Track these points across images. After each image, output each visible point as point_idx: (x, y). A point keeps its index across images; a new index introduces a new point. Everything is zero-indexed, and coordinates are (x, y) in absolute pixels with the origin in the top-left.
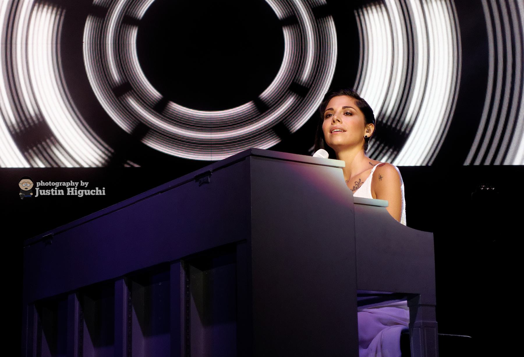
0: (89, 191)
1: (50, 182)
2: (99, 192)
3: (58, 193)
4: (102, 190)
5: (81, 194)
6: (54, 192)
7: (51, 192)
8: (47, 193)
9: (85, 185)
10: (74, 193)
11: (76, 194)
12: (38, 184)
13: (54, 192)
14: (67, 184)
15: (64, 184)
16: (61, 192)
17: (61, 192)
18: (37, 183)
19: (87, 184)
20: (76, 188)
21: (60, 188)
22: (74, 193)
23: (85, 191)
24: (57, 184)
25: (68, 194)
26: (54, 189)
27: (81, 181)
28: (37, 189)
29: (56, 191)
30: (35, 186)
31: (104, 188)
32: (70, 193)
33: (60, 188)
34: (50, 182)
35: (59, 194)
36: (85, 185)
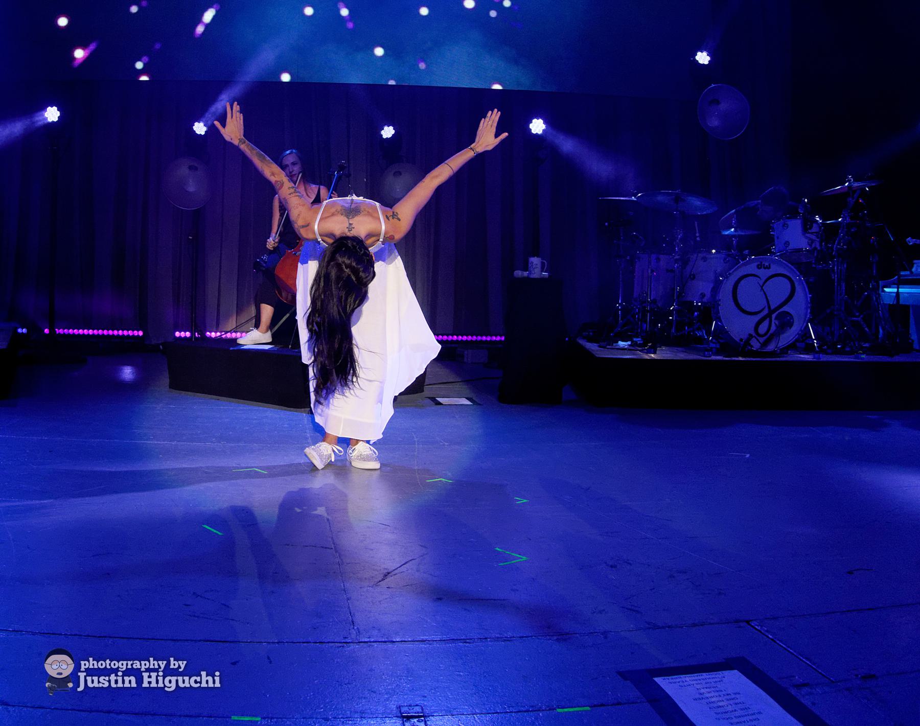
1: (108, 661)
9: (179, 667)
12: (84, 665)
14: (144, 665)
15: (137, 665)
18: (83, 663)
19: (183, 664)
24: (123, 665)
27: (172, 659)
34: (108, 661)
36: (179, 667)
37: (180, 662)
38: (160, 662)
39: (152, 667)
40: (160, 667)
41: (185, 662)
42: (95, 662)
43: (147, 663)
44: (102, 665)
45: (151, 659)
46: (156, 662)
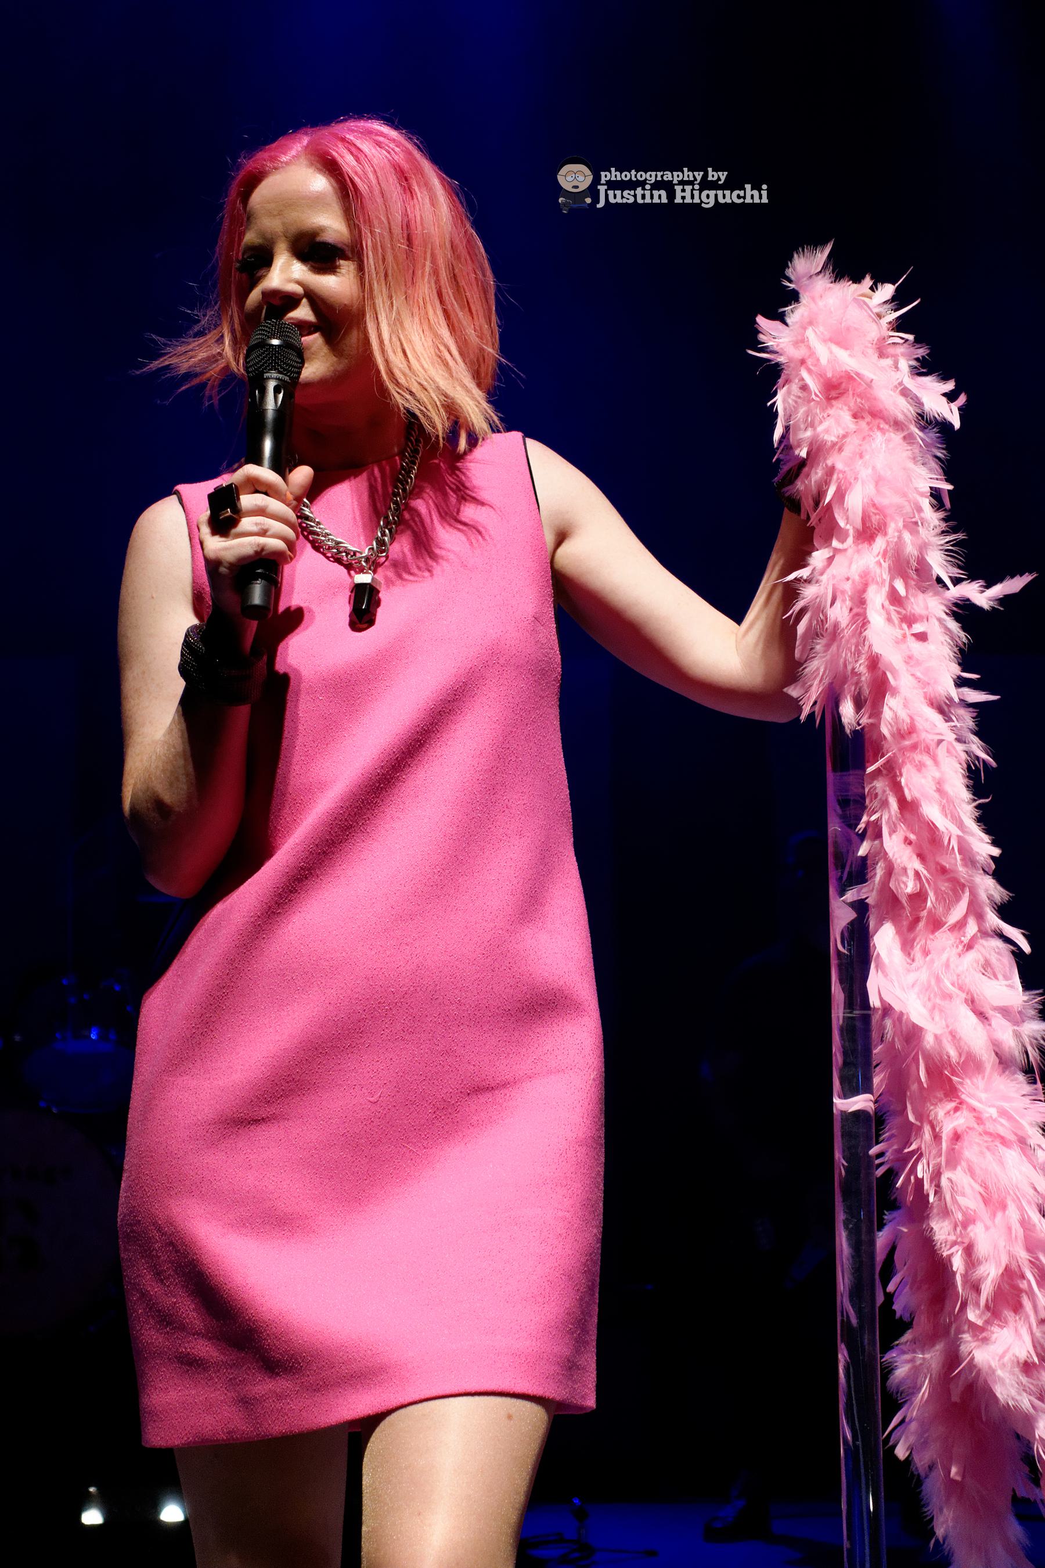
0: (727, 193)
1: (633, 172)
2: (753, 195)
3: (652, 197)
4: (760, 190)
5: (708, 199)
6: (643, 196)
7: (635, 196)
8: (627, 197)
9: (719, 179)
10: (692, 197)
11: (697, 200)
12: (605, 176)
13: (643, 197)
14: (676, 177)
15: (668, 176)
16: (661, 197)
17: (660, 197)
18: (603, 174)
19: (723, 176)
20: (697, 187)
21: (657, 185)
22: (692, 197)
23: (720, 193)
24: (651, 177)
25: (678, 200)
26: (644, 189)
27: (710, 169)
28: (602, 189)
29: (648, 193)
30: (596, 180)
31: (765, 187)
32: (683, 198)
33: (657, 185)
34: (633, 172)
35: (656, 200)
36: (719, 179)
37: (720, 173)
38: (696, 173)
39: (686, 178)
40: (695, 179)
41: (726, 173)
42: (618, 173)
43: (680, 174)
44: (626, 176)
45: (685, 169)
46: (691, 173)
